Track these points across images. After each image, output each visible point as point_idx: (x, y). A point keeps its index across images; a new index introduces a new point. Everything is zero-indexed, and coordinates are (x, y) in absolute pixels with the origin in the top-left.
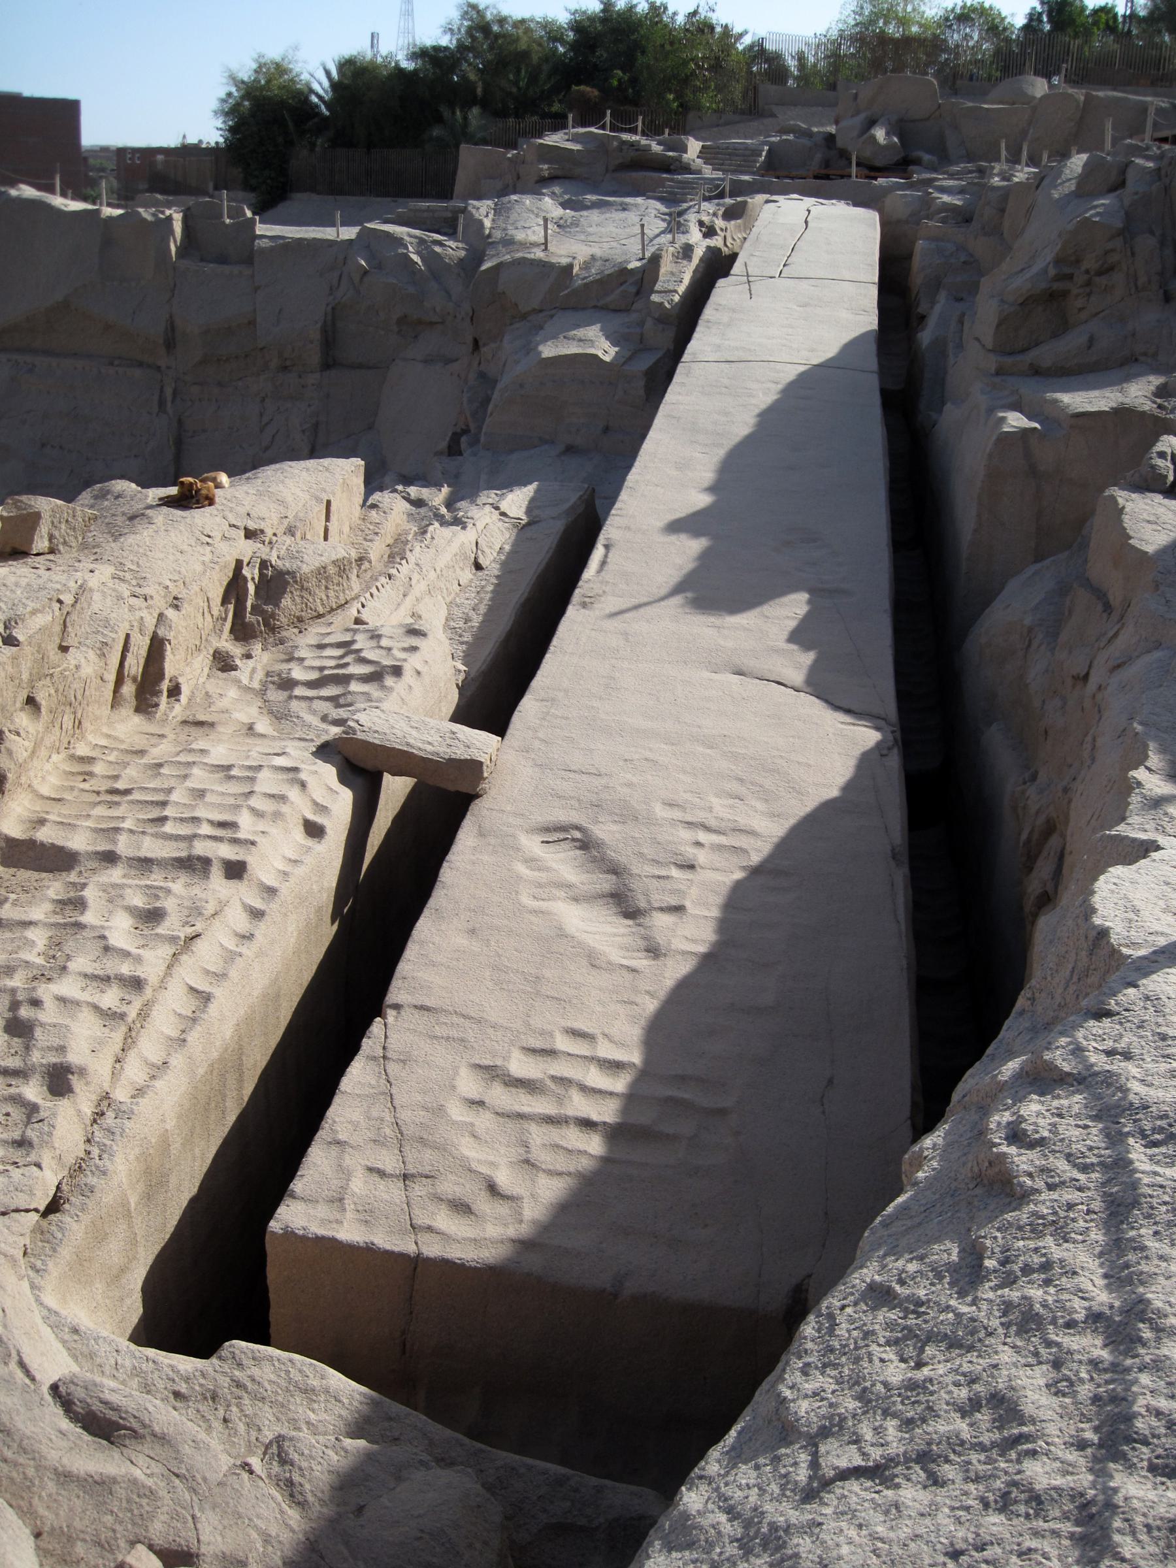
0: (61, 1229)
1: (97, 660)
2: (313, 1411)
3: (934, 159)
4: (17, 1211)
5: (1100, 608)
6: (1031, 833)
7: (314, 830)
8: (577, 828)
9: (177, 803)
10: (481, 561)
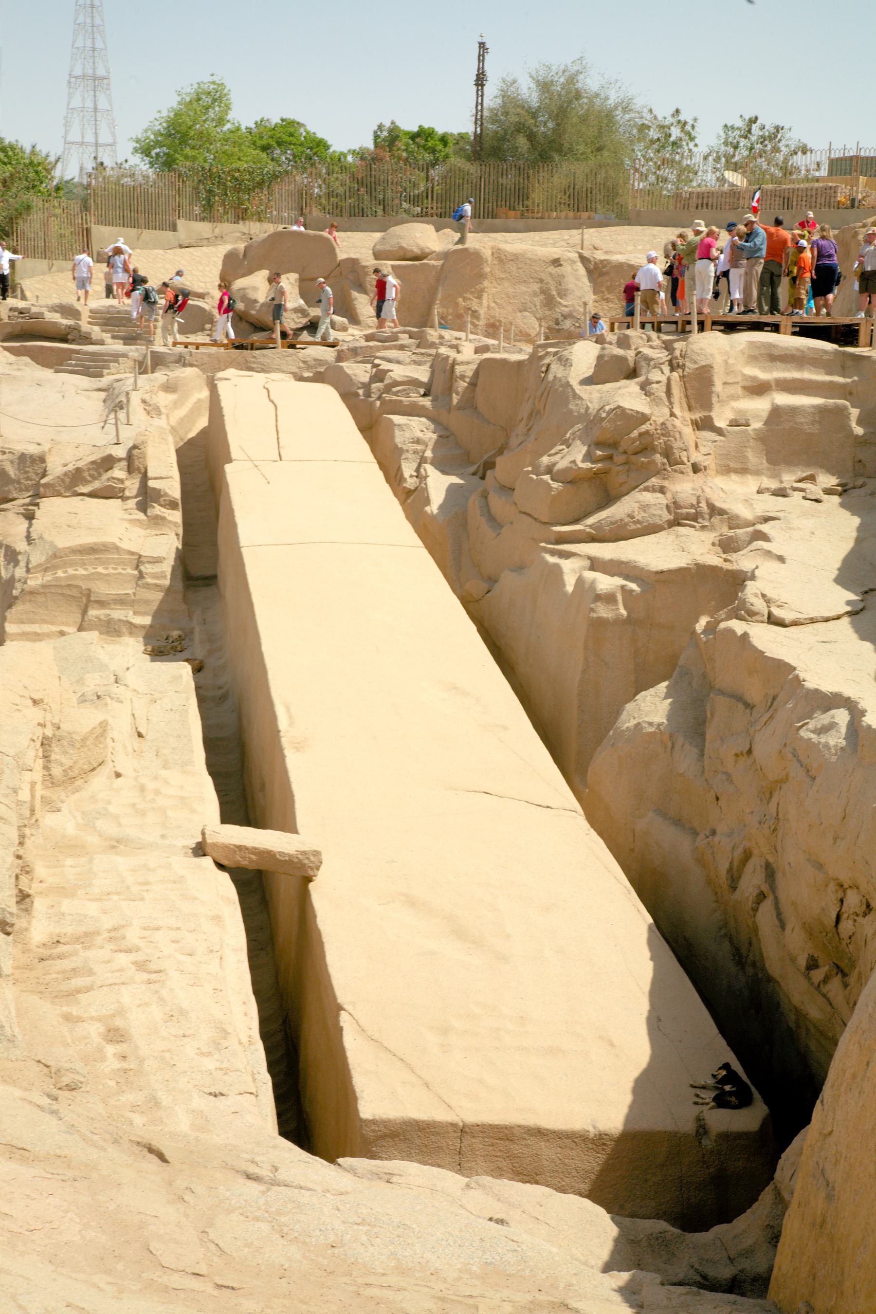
3: (345, 320)
5: (741, 706)
6: (731, 863)
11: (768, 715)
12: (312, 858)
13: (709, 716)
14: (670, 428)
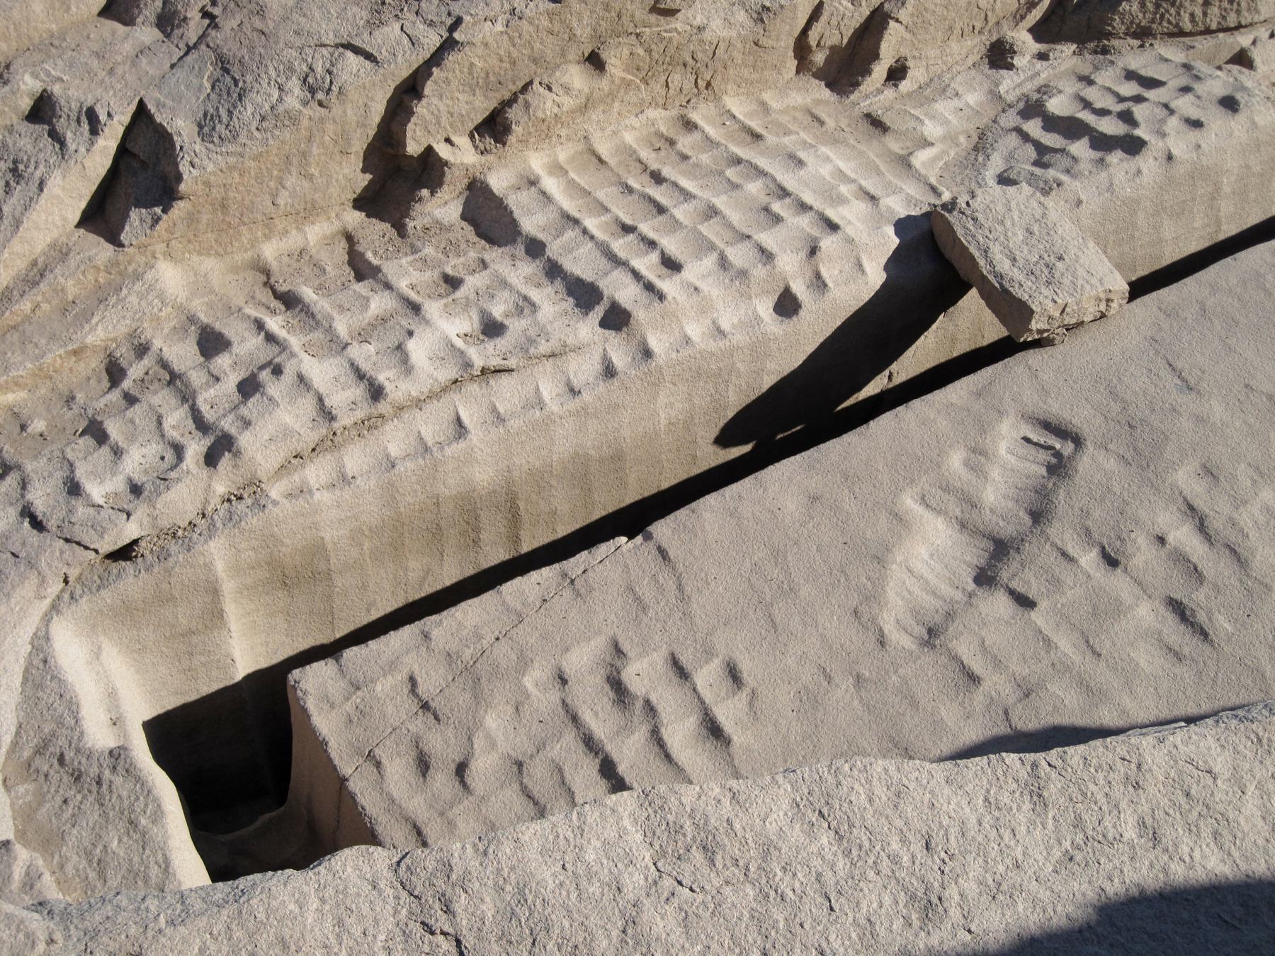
0: (119, 575)
1: (749, 24)
2: (120, 841)
4: (78, 543)
7: (787, 305)
8: (1078, 441)
9: (673, 216)
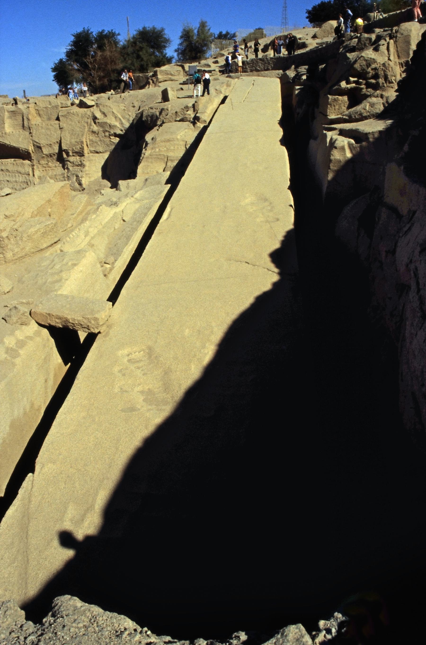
10: (124, 218)
11: (408, 226)
12: (93, 322)
13: (377, 220)
14: (387, 65)
